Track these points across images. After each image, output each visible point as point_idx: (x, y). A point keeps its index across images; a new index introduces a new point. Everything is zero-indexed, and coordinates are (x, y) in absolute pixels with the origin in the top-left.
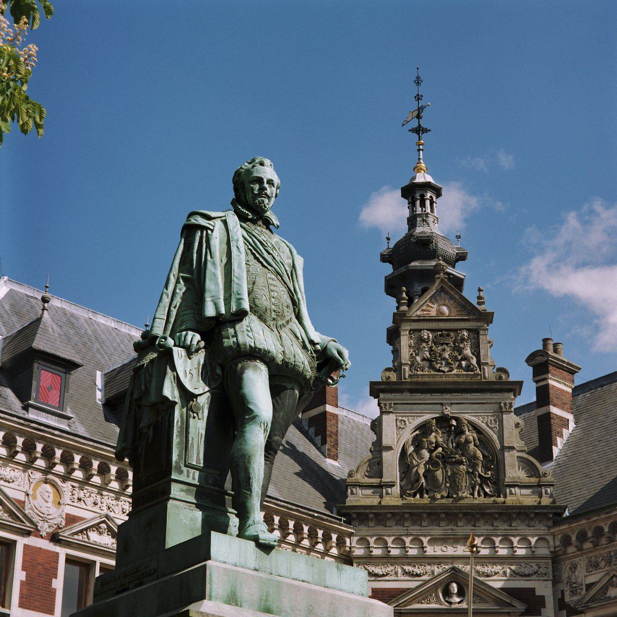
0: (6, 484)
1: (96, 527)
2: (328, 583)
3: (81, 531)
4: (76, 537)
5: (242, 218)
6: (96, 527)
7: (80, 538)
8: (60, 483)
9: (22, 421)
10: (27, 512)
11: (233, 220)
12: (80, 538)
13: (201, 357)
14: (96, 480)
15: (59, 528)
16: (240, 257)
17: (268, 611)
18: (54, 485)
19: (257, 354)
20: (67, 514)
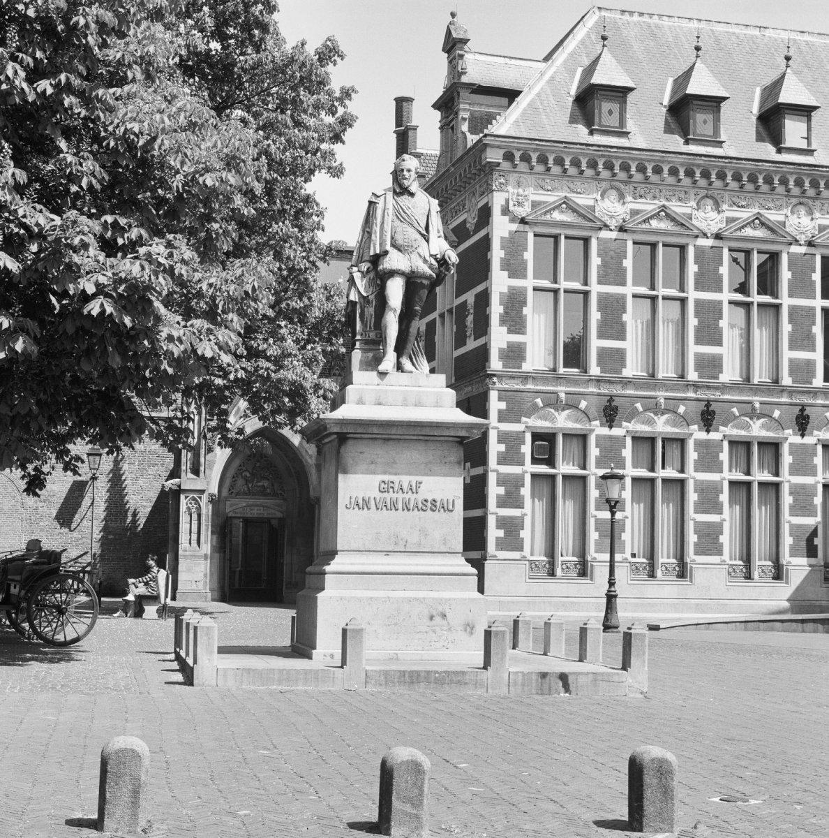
0: (579, 195)
1: (656, 216)
2: (420, 384)
3: (644, 221)
4: (640, 226)
5: (395, 192)
6: (656, 216)
7: (644, 226)
8: (623, 187)
9: (584, 147)
10: (597, 215)
11: (390, 195)
12: (644, 226)
13: (372, 275)
14: (654, 178)
15: (624, 221)
16: (388, 220)
17: (380, 404)
18: (618, 189)
19: (392, 273)
20: (631, 210)
